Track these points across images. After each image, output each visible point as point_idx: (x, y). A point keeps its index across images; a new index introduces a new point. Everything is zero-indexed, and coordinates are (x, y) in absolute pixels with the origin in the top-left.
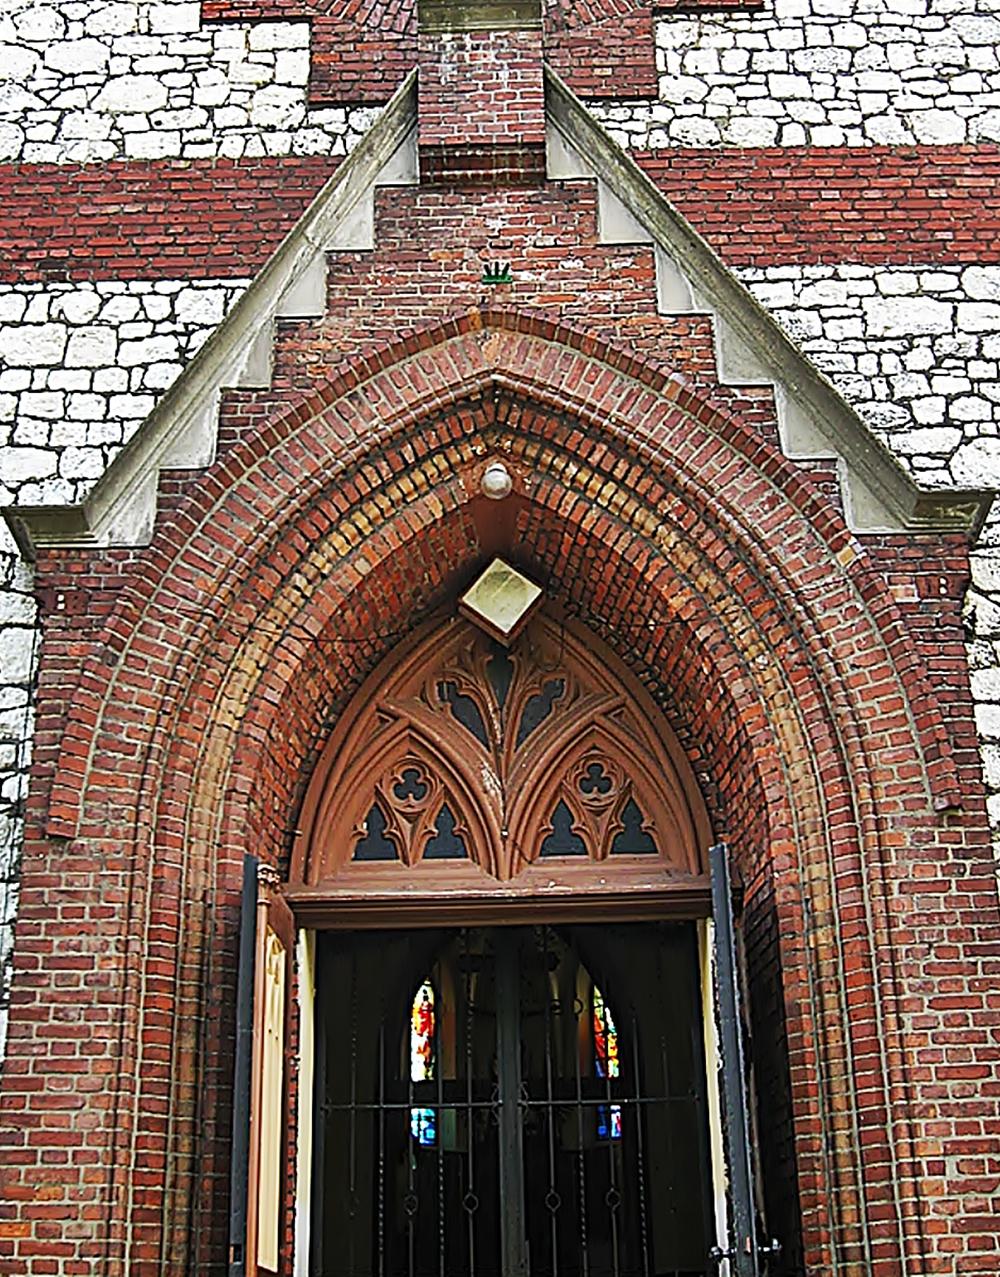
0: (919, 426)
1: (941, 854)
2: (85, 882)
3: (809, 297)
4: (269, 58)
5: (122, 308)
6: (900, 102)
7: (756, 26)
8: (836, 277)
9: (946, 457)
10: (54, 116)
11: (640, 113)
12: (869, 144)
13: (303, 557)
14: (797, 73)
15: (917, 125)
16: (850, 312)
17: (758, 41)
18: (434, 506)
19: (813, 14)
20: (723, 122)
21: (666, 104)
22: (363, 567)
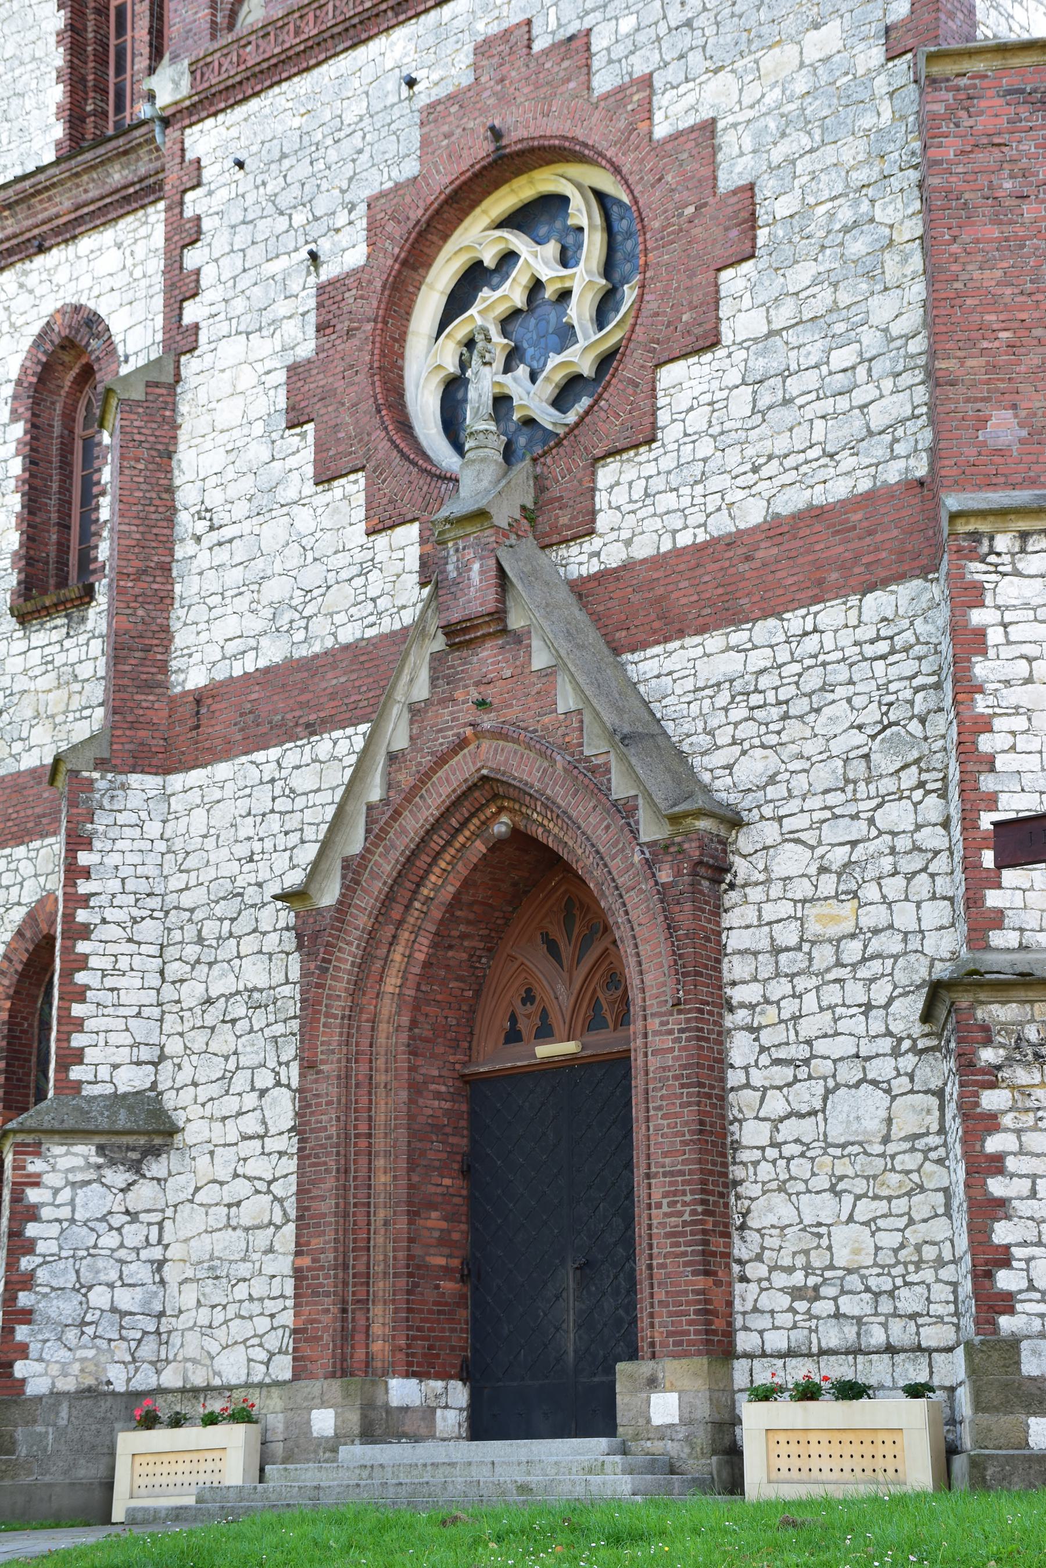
0: (718, 748)
1: (670, 1032)
2: (323, 1088)
3: (669, 665)
4: (400, 554)
5: (343, 747)
6: (728, 499)
8: (682, 647)
9: (730, 767)
10: (303, 623)
13: (415, 892)
18: (480, 847)
20: (628, 543)
22: (451, 889)
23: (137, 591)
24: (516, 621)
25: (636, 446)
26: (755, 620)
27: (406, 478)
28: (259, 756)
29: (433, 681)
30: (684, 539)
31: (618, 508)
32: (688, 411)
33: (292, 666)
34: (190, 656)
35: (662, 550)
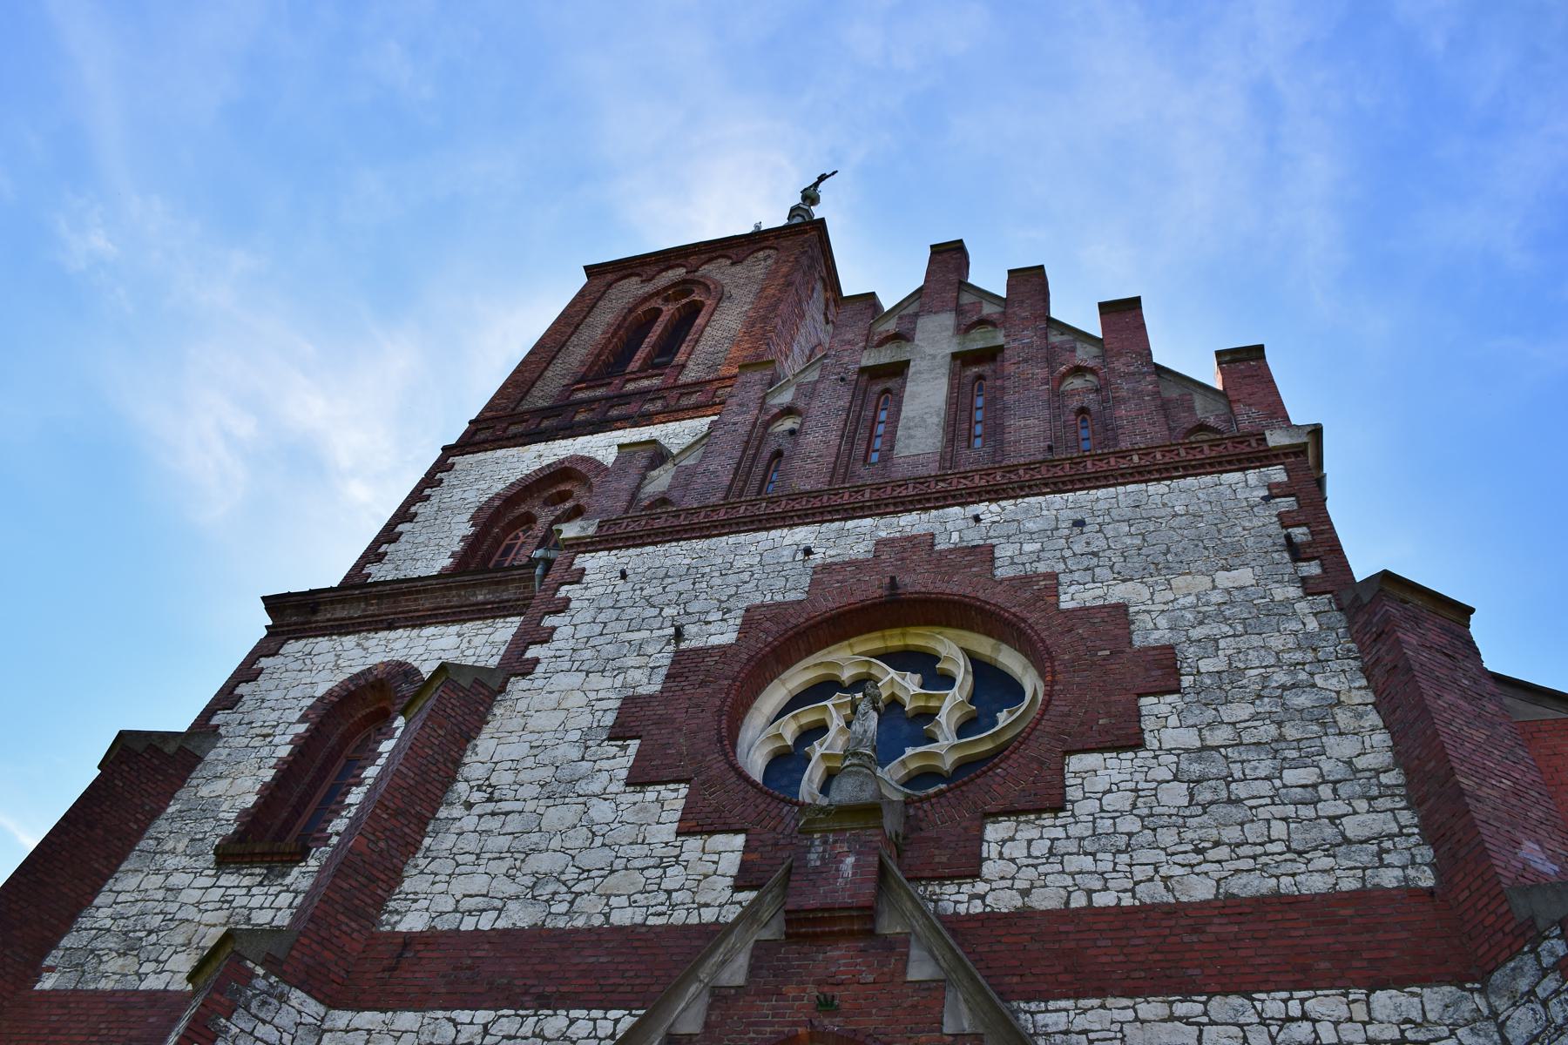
3: (1081, 1022)
4: (715, 857)
6: (1164, 871)
7: (1058, 822)
8: (1103, 1007)
10: (569, 897)
11: (965, 888)
12: (1137, 903)
14: (1086, 854)
15: (1177, 887)
16: (1112, 1035)
17: (1060, 833)
19: (1102, 810)
20: (1025, 893)
21: (986, 881)
23: (388, 825)
24: (889, 926)
25: (1039, 811)
26: (1211, 995)
27: (741, 794)
28: (463, 1016)
29: (753, 970)
30: (1103, 900)
31: (1013, 860)
32: (1104, 793)
33: (538, 934)
34: (415, 901)
35: (1073, 905)
